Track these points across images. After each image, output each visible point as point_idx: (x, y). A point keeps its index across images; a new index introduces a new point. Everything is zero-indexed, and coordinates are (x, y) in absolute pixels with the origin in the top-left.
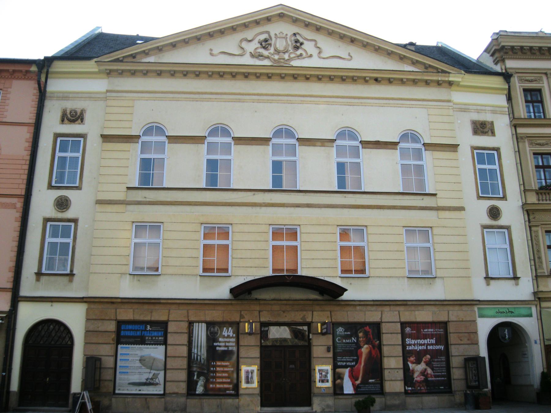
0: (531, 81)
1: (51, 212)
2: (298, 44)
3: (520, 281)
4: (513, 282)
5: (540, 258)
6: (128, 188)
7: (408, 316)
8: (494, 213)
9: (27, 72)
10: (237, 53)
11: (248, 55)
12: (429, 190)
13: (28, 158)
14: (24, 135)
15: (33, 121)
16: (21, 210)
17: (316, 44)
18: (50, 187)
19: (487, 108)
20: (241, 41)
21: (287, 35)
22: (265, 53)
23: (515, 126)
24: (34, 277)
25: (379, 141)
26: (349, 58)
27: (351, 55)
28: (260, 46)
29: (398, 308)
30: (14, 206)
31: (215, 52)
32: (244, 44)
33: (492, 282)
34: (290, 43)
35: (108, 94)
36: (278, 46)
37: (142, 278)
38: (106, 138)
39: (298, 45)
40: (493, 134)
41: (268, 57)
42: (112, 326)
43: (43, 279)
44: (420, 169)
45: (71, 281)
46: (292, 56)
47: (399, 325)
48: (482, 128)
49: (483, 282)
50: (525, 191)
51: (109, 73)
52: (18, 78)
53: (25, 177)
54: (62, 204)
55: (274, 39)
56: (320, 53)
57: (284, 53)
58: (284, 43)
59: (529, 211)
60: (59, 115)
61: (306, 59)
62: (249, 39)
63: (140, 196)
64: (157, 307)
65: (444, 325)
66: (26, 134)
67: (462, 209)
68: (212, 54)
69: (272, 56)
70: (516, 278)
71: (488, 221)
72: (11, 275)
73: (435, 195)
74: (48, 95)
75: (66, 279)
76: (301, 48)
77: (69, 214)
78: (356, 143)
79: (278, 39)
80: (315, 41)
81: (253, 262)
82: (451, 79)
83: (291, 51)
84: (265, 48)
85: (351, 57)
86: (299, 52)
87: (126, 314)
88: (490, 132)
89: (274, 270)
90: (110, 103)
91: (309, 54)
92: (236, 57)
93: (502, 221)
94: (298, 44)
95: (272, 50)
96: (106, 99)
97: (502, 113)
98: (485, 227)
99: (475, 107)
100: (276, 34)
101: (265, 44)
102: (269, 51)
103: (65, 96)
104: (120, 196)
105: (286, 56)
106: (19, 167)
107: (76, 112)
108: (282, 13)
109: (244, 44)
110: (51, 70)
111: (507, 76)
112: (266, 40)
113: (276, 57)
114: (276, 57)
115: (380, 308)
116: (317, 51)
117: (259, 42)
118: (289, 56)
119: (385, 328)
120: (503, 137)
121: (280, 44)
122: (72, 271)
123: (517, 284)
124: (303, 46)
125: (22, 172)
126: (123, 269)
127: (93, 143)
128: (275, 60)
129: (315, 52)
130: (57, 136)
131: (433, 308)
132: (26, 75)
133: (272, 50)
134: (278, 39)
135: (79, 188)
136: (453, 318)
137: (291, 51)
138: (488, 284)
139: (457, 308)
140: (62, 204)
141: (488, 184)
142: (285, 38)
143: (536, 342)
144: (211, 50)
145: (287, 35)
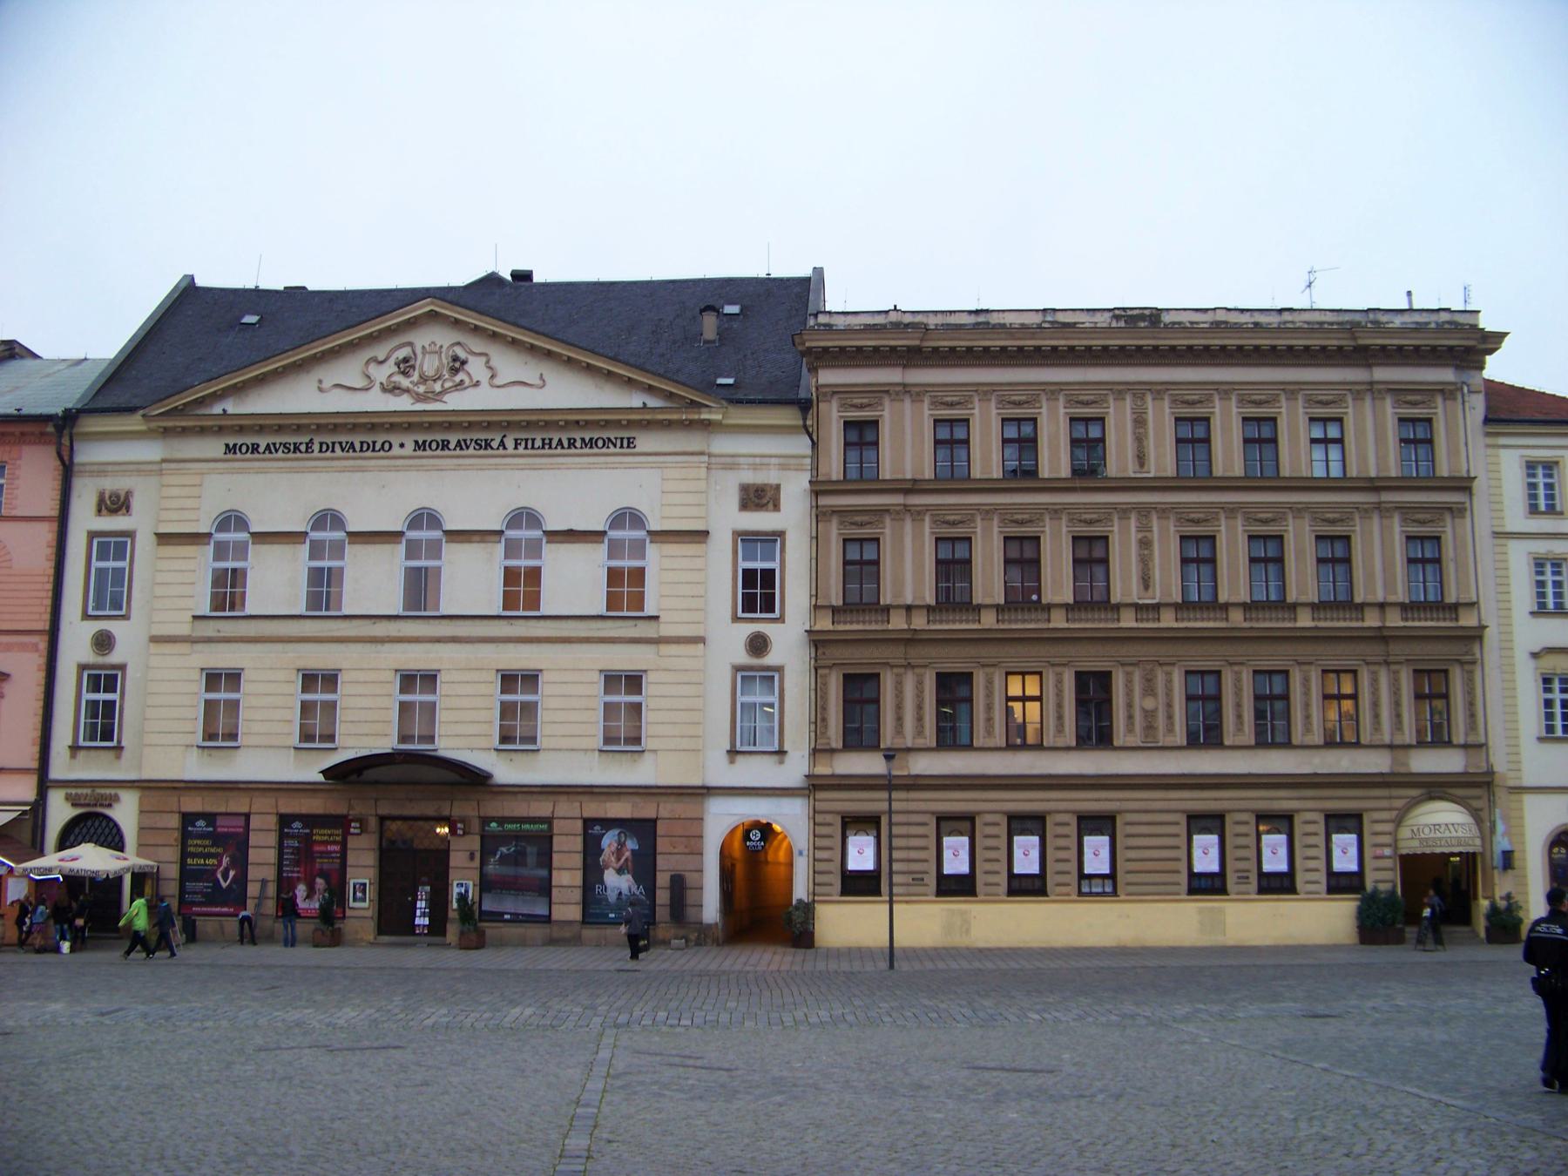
0: (861, 407)
1: (88, 655)
2: (457, 365)
3: (788, 759)
4: (775, 758)
5: (824, 720)
6: (195, 617)
7: (594, 809)
8: (758, 645)
9: (42, 434)
11: (377, 385)
12: (649, 610)
13: (52, 571)
14: (45, 534)
15: (55, 513)
16: (45, 653)
18: (86, 616)
19: (773, 461)
20: (367, 363)
22: (405, 382)
23: (816, 493)
24: (68, 752)
25: (571, 531)
26: (539, 382)
29: (581, 798)
30: (35, 648)
31: (326, 385)
32: (373, 370)
33: (740, 759)
35: (164, 465)
37: (214, 752)
38: (164, 538)
39: (457, 365)
40: (777, 507)
41: (407, 391)
42: (174, 821)
43: (81, 754)
44: (638, 575)
45: (118, 757)
46: (448, 385)
47: (580, 824)
48: (757, 497)
49: (724, 758)
50: (816, 607)
51: (166, 432)
52: (30, 443)
53: (49, 602)
54: (104, 642)
56: (492, 377)
59: (818, 641)
60: (92, 501)
62: (381, 358)
63: (209, 629)
64: (235, 793)
65: (652, 823)
66: (47, 533)
67: (700, 640)
68: (321, 390)
70: (781, 753)
71: (743, 658)
72: (36, 749)
73: (656, 618)
74: (76, 468)
75: (111, 754)
77: (115, 658)
78: (538, 533)
81: (367, 729)
82: (704, 416)
84: (405, 374)
86: (458, 379)
87: (193, 804)
88: (771, 506)
89: (403, 738)
90: (167, 480)
93: (770, 659)
94: (457, 365)
95: (416, 377)
96: (160, 473)
97: (799, 469)
98: (737, 669)
99: (751, 460)
101: (406, 366)
103: (102, 469)
104: (184, 629)
105: (437, 387)
106: (39, 586)
107: (118, 497)
110: (75, 430)
111: (805, 406)
112: (406, 360)
113: (421, 389)
114: (421, 389)
115: (551, 798)
119: (558, 826)
120: (792, 514)
121: (429, 365)
122: (119, 741)
123: (781, 762)
124: (466, 367)
125: (43, 594)
126: (190, 739)
127: (144, 545)
130: (92, 535)
131: (637, 799)
132: (42, 439)
133: (416, 377)
135: (126, 617)
136: (664, 813)
138: (732, 762)
139: (672, 798)
140: (104, 642)
141: (758, 592)
143: (801, 853)
144: (320, 381)
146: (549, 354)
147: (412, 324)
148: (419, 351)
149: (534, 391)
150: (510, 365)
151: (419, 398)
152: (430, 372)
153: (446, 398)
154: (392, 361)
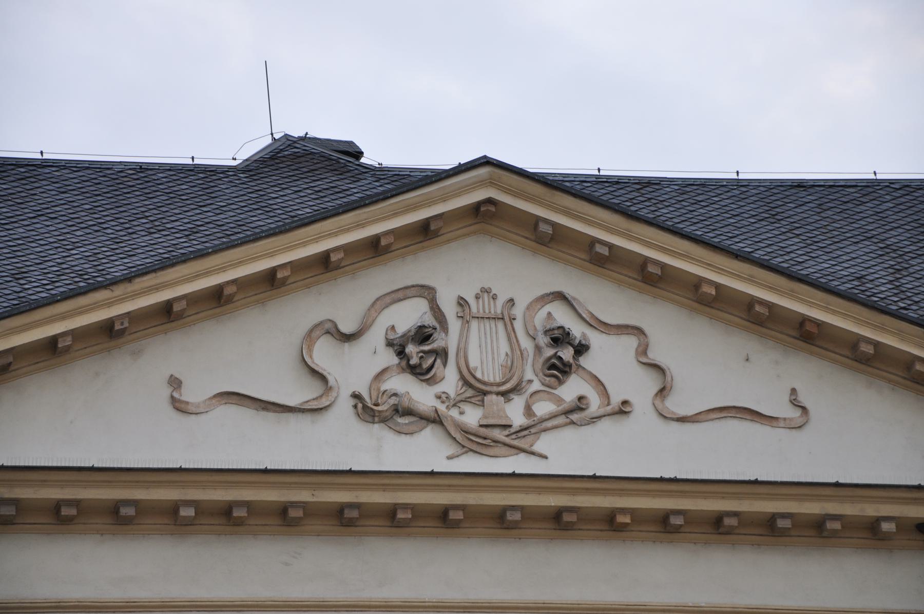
10: (296, 393)
11: (344, 405)
17: (643, 350)
20: (310, 337)
21: (511, 301)
26: (795, 413)
27: (803, 399)
28: (395, 360)
31: (192, 394)
32: (324, 355)
34: (526, 344)
36: (474, 361)
39: (562, 355)
41: (435, 420)
46: (543, 408)
55: (454, 325)
56: (662, 392)
57: (503, 394)
58: (504, 347)
61: (605, 424)
68: (179, 406)
69: (454, 413)
76: (579, 366)
79: (474, 324)
80: (638, 331)
83: (536, 386)
84: (420, 372)
85: (804, 409)
91: (616, 400)
92: (291, 417)
94: (567, 354)
95: (450, 382)
100: (462, 303)
101: (418, 351)
102: (438, 388)
105: (514, 412)
108: (490, 201)
109: (324, 355)
112: (422, 335)
113: (472, 417)
114: (472, 417)
116: (650, 383)
117: (390, 344)
118: (528, 411)
124: (584, 361)
128: (466, 431)
129: (633, 385)
133: (450, 382)
134: (474, 324)
137: (536, 386)
142: (505, 319)
144: (175, 383)
145: (511, 301)
146: (807, 336)
147: (426, 233)
148: (450, 309)
149: (780, 433)
150: (709, 362)
151: (473, 440)
152: (489, 370)
153: (540, 445)
154: (376, 336)
